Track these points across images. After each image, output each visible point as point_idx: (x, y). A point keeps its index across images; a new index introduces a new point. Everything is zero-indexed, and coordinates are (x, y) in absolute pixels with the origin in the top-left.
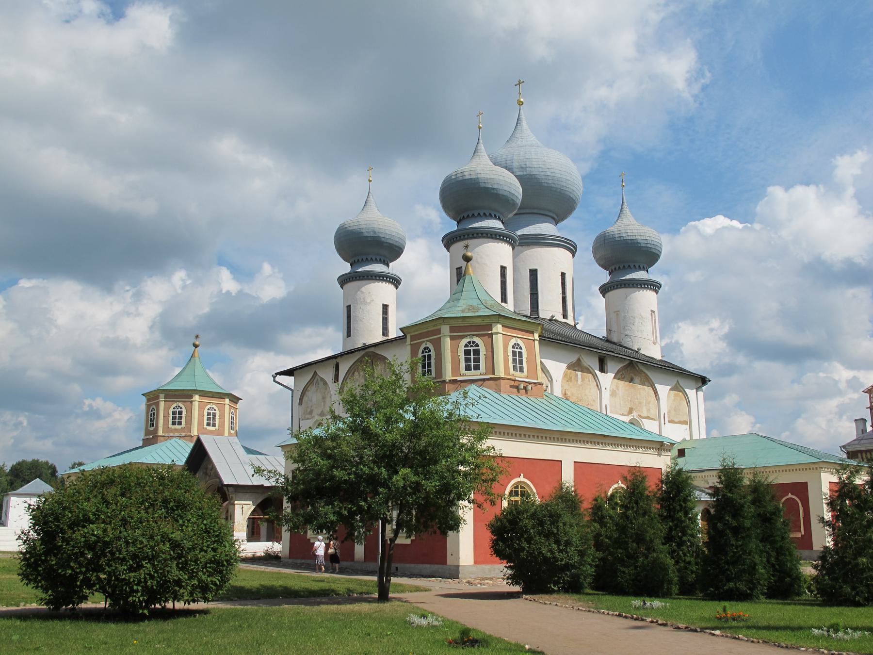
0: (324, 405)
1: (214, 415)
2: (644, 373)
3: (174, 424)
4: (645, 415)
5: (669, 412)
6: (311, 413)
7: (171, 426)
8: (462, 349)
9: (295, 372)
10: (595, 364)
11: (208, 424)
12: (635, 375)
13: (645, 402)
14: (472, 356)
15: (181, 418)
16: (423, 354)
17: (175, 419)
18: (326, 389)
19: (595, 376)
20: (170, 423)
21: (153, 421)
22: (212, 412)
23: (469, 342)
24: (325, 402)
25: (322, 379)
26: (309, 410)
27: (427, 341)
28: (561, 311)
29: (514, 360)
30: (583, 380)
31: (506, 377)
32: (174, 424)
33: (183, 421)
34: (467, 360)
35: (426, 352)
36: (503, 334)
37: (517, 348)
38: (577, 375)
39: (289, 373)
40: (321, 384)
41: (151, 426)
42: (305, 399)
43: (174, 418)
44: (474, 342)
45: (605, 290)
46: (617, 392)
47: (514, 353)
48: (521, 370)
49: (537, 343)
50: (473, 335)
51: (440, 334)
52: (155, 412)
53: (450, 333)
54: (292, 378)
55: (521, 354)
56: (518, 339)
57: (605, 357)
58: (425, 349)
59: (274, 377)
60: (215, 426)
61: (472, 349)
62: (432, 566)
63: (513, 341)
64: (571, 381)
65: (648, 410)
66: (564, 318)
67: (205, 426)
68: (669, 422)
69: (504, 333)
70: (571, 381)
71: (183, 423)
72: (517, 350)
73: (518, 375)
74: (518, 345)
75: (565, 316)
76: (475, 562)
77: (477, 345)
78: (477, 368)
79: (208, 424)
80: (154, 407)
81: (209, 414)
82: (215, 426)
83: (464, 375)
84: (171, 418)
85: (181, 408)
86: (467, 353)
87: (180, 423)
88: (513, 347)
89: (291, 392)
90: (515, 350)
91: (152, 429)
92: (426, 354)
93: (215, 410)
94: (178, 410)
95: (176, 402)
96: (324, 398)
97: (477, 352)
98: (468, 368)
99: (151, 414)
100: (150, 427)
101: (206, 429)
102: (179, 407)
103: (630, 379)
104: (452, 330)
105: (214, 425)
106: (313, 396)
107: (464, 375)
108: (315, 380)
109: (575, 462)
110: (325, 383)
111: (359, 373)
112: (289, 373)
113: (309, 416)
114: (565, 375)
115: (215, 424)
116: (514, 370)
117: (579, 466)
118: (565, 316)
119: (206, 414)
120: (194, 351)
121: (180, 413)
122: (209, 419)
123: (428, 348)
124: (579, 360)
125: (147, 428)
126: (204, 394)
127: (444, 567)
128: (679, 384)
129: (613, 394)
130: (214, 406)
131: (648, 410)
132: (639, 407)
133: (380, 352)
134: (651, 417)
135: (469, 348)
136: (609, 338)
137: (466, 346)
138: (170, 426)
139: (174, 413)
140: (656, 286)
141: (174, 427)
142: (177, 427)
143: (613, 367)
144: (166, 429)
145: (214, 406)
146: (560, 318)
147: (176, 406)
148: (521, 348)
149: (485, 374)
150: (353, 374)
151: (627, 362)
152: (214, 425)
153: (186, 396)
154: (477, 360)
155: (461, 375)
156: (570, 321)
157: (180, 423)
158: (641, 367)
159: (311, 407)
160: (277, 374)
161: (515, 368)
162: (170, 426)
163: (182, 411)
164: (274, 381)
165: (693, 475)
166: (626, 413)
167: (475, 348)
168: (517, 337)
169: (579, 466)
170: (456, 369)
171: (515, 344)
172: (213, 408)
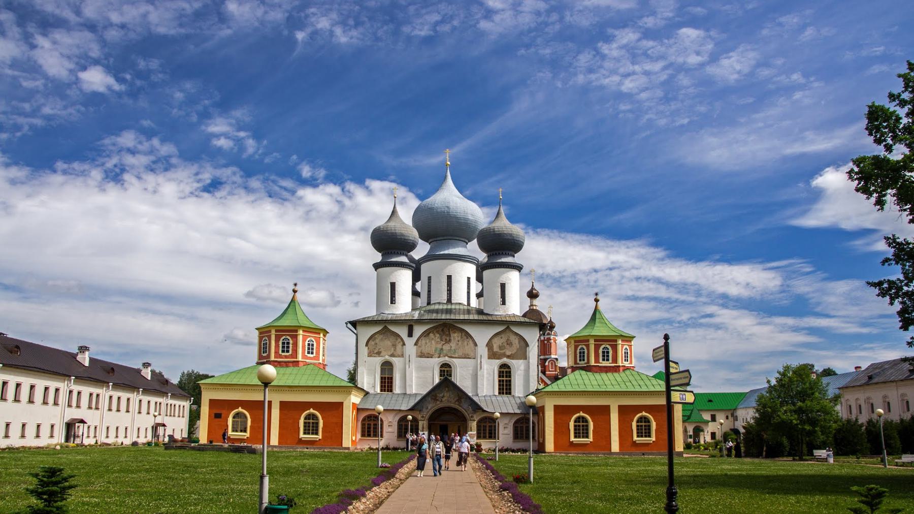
3: (308, 353)
8: (601, 350)
15: (313, 349)
20: (306, 352)
32: (308, 353)
33: (314, 351)
34: (603, 356)
39: (354, 324)
43: (309, 349)
71: (314, 353)
78: (608, 360)
83: (602, 363)
85: (313, 342)
86: (603, 352)
87: (312, 353)
89: (355, 336)
94: (311, 343)
97: (608, 352)
98: (603, 360)
119: (306, 344)
120: (294, 297)
121: (313, 345)
126: (308, 330)
130: (288, 337)
133: (468, 329)
137: (603, 349)
138: (306, 354)
139: (309, 344)
142: (310, 355)
144: (304, 356)
153: (292, 332)
155: (600, 363)
157: (312, 353)
162: (306, 354)
170: (597, 361)
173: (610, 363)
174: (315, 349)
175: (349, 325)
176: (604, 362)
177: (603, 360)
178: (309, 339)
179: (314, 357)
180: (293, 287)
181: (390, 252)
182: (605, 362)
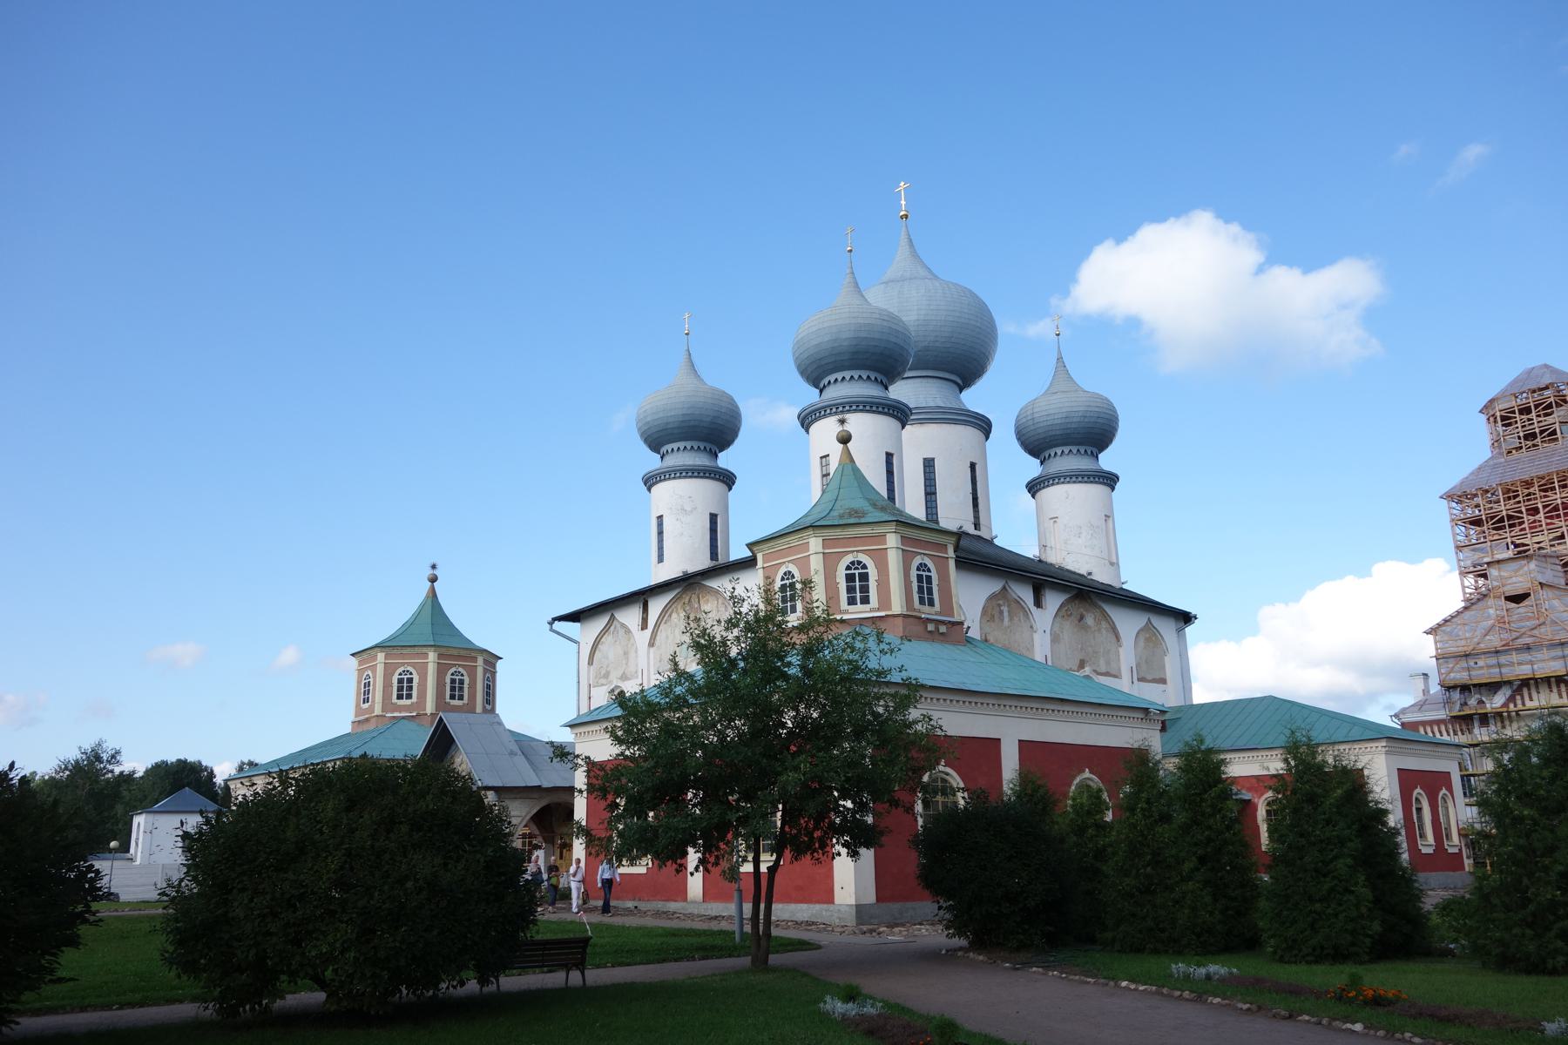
0: (627, 664)
1: (462, 682)
2: (1100, 607)
3: (400, 697)
4: (1103, 670)
5: (1138, 665)
6: (607, 675)
7: (396, 701)
9: (582, 616)
10: (1025, 594)
11: (452, 697)
12: (1087, 611)
13: (1102, 650)
14: (857, 584)
15: (410, 688)
16: (783, 582)
17: (402, 690)
18: (629, 640)
19: (1027, 613)
20: (395, 696)
21: (368, 694)
22: (457, 678)
23: (853, 563)
24: (627, 659)
25: (623, 625)
26: (603, 672)
27: (788, 562)
28: (972, 519)
29: (920, 589)
30: (1011, 619)
31: (908, 613)
32: (400, 697)
33: (415, 693)
34: (850, 590)
35: (788, 579)
36: (903, 550)
37: (924, 571)
38: (1001, 612)
39: (575, 617)
40: (622, 632)
41: (366, 701)
42: (598, 655)
43: (400, 689)
44: (859, 563)
45: (1034, 487)
46: (1061, 637)
47: (920, 578)
48: (931, 603)
49: (952, 563)
50: (857, 551)
51: (809, 551)
52: (371, 680)
53: (823, 548)
54: (577, 625)
55: (929, 579)
56: (926, 558)
57: (1042, 584)
58: (785, 574)
59: (551, 624)
60: (462, 699)
61: (857, 572)
62: (812, 906)
63: (917, 561)
64: (994, 621)
65: (1108, 663)
66: (976, 529)
67: (448, 700)
68: (1139, 680)
69: (904, 548)
70: (994, 621)
72: (924, 574)
73: (926, 612)
74: (926, 565)
75: (977, 526)
76: (879, 899)
77: (865, 567)
78: (865, 600)
79: (452, 697)
80: (370, 673)
81: (453, 681)
82: (462, 699)
83: (847, 612)
84: (395, 689)
85: (411, 674)
86: (850, 578)
87: (409, 696)
88: (918, 569)
90: (921, 573)
91: (366, 705)
92: (787, 582)
93: (462, 675)
95: (403, 664)
96: (626, 653)
97: (864, 577)
98: (852, 601)
99: (365, 683)
100: (364, 703)
101: (449, 703)
102: (408, 671)
103: (1079, 617)
104: (826, 543)
105: (461, 698)
106: (609, 648)
107: (847, 612)
108: (612, 628)
109: (1019, 741)
110: (628, 631)
111: (678, 614)
112: (575, 617)
113: (603, 681)
114: (985, 611)
115: (462, 696)
116: (920, 603)
117: (1025, 746)
118: (977, 526)
119: (448, 681)
121: (410, 681)
122: (453, 689)
123: (790, 572)
124: (1004, 588)
125: (358, 705)
127: (831, 907)
128: (1151, 623)
129: (1055, 639)
130: (460, 669)
131: (1108, 663)
132: (1093, 659)
134: (1113, 672)
135: (853, 571)
136: (1043, 558)
137: (848, 568)
139: (400, 681)
140: (1107, 478)
141: (401, 702)
142: (405, 702)
143: (1053, 601)
145: (460, 669)
146: (971, 530)
147: (404, 671)
148: (929, 570)
149: (878, 610)
150: (670, 616)
151: (1075, 592)
152: (461, 698)
154: (865, 589)
155: (841, 612)
156: (983, 533)
157: (409, 696)
158: (1093, 596)
159: (607, 667)
160: (555, 619)
161: (922, 601)
163: (412, 678)
164: (552, 630)
165: (1228, 756)
166: (1076, 669)
167: (861, 571)
168: (924, 554)
169: (1025, 746)
171: (921, 564)
172: (459, 672)
173: (871, 611)
174: (415, 689)
175: (558, 625)
176: (852, 608)
177: (849, 604)
178: (400, 670)
179: (464, 704)
180: (430, 572)
181: (675, 449)
182: (859, 607)
